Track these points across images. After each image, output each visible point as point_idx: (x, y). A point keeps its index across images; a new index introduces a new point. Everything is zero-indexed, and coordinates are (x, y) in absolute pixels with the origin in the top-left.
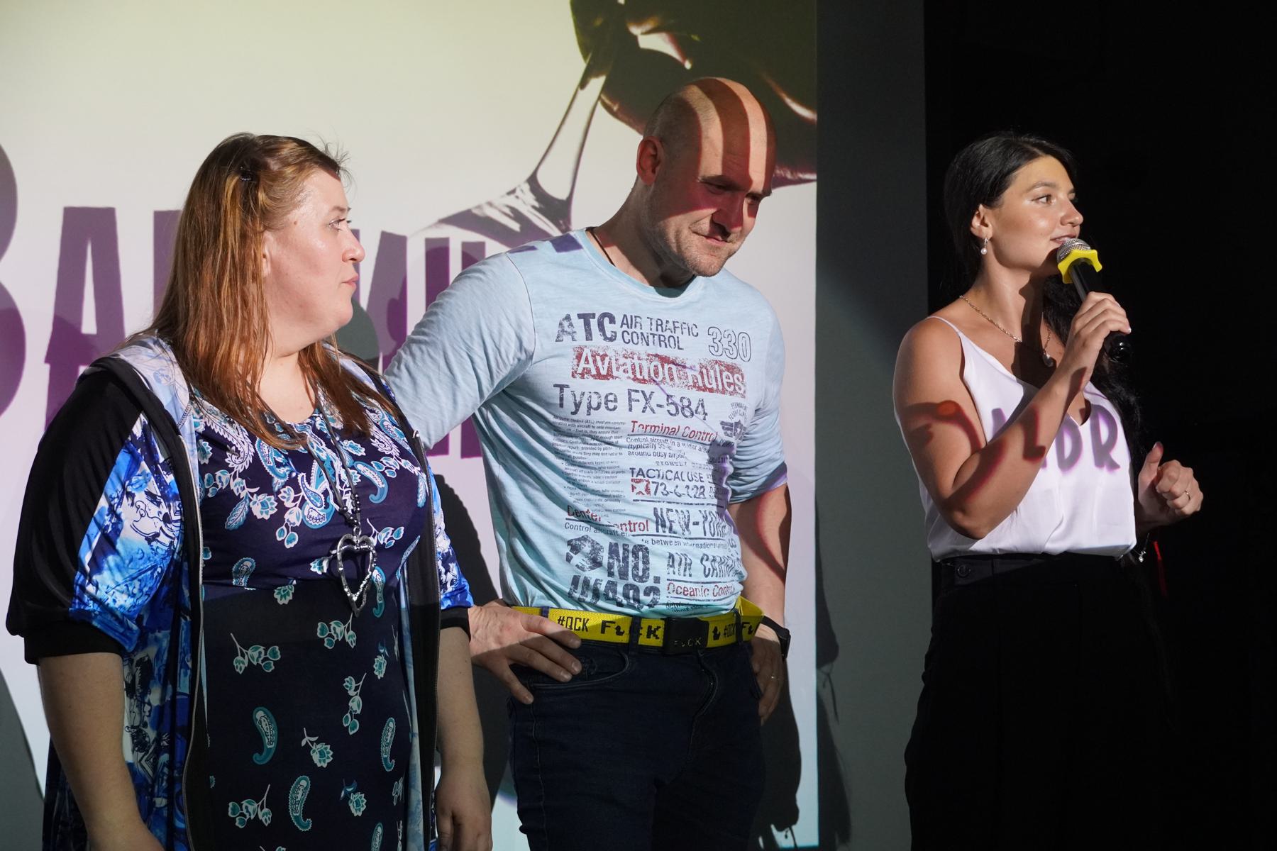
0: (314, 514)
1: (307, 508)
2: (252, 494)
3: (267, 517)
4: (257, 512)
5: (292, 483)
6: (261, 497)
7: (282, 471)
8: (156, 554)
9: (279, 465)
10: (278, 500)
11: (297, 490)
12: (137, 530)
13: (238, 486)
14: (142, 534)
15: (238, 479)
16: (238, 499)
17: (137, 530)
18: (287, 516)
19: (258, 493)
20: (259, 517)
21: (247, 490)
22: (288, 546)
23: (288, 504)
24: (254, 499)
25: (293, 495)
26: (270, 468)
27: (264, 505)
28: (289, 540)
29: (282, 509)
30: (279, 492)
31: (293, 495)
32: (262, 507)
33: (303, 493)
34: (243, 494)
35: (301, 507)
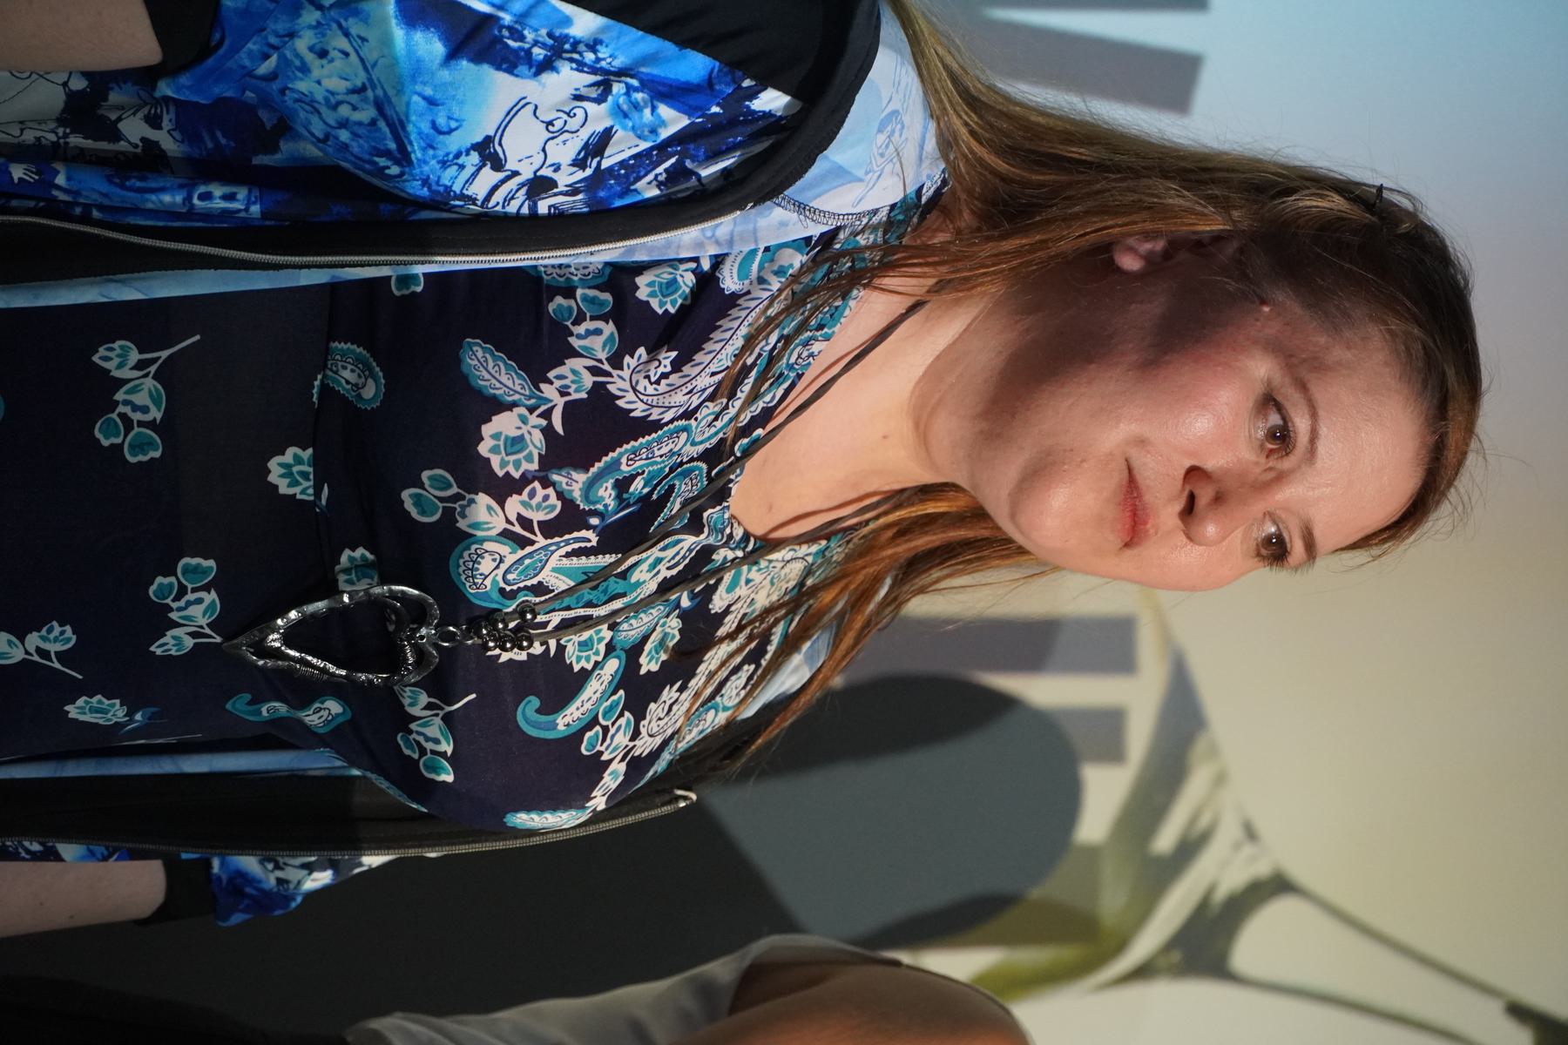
0: (486, 565)
1: (504, 549)
2: (547, 415)
3: (483, 449)
4: (503, 424)
5: (570, 518)
6: (538, 437)
7: (606, 494)
8: (444, 164)
9: (622, 485)
10: (526, 480)
11: (549, 529)
12: (511, 114)
13: (572, 379)
14: (502, 128)
15: (588, 380)
16: (537, 376)
17: (511, 114)
18: (483, 499)
19: (548, 431)
20: (487, 430)
21: (560, 402)
22: (406, 495)
23: (514, 505)
24: (534, 420)
25: (537, 517)
26: (617, 462)
27: (516, 444)
28: (422, 499)
29: (503, 489)
30: (546, 483)
31: (537, 517)
32: (510, 437)
33: (541, 541)
34: (549, 391)
35: (506, 535)
